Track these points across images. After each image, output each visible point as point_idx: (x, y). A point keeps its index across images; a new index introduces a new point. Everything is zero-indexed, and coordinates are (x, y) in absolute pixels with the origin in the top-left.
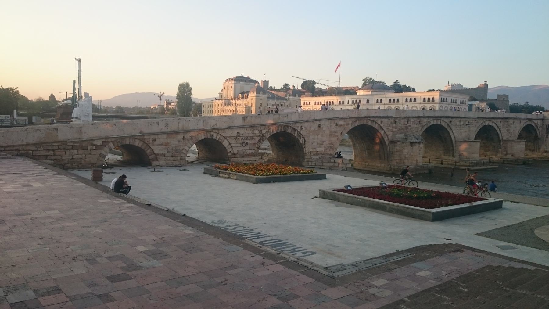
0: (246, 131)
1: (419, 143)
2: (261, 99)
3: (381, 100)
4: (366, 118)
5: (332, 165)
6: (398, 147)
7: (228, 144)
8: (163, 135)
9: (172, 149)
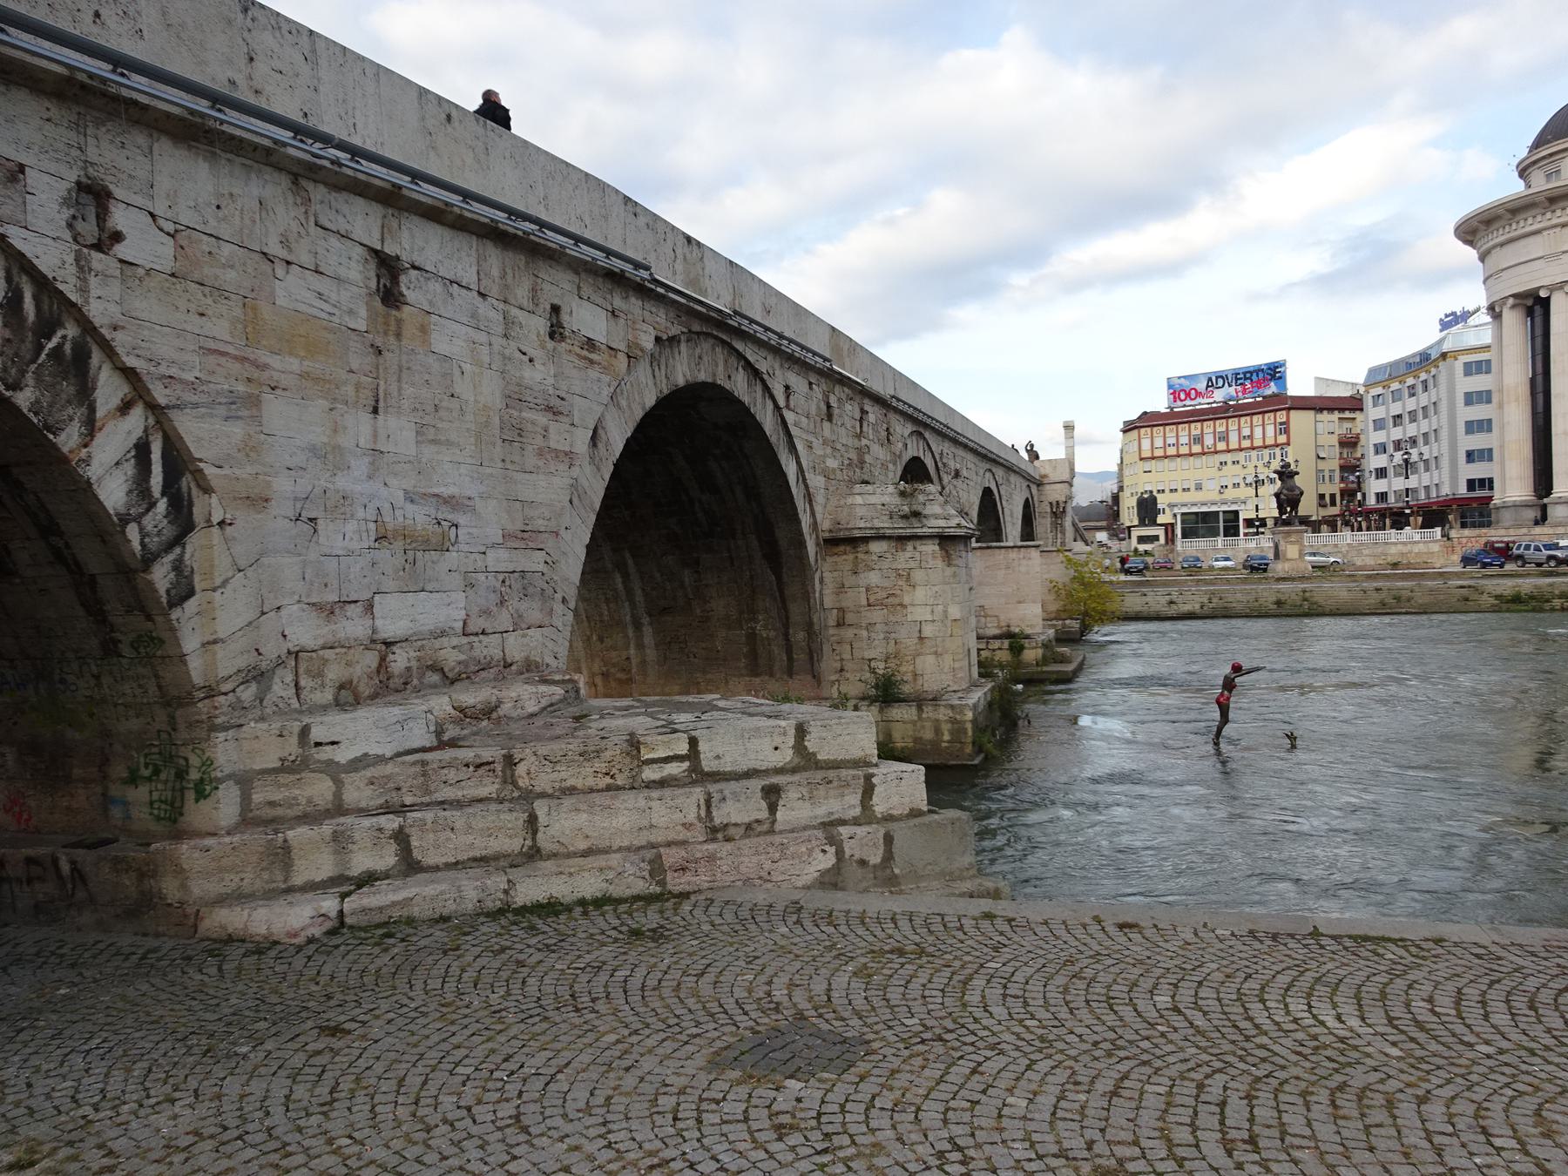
6: (878, 569)
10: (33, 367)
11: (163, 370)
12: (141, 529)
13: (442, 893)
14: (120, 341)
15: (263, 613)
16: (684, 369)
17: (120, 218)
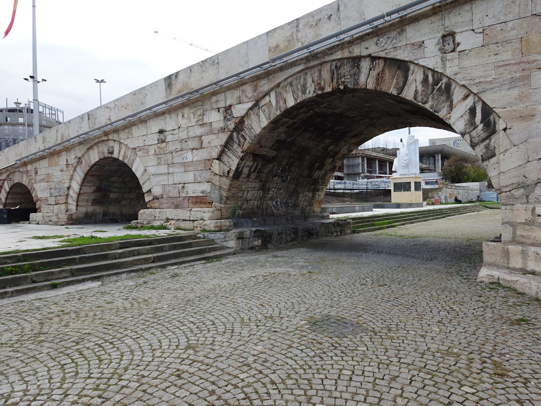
0: (183, 122)
8: (44, 160)
9: (56, 189)
10: (431, 95)
11: (477, 81)
12: (470, 136)
13: (525, 283)
14: (458, 78)
15: (529, 162)
17: (458, 38)
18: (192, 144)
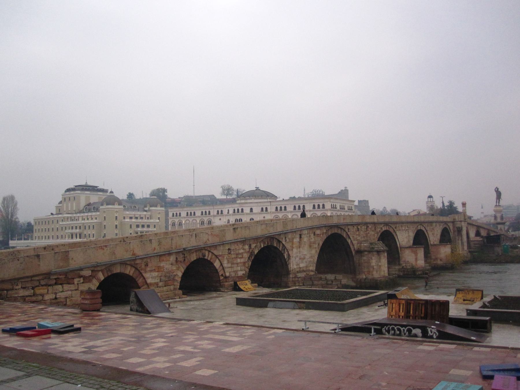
0: (237, 247)
1: (383, 251)
2: (117, 212)
3: (266, 208)
4: (337, 226)
5: (324, 282)
7: (219, 264)
16: (330, 233)
18: (240, 256)
